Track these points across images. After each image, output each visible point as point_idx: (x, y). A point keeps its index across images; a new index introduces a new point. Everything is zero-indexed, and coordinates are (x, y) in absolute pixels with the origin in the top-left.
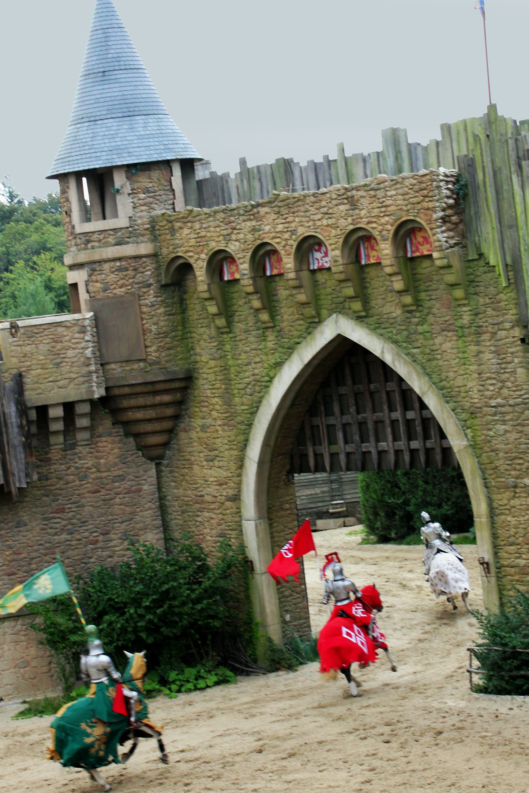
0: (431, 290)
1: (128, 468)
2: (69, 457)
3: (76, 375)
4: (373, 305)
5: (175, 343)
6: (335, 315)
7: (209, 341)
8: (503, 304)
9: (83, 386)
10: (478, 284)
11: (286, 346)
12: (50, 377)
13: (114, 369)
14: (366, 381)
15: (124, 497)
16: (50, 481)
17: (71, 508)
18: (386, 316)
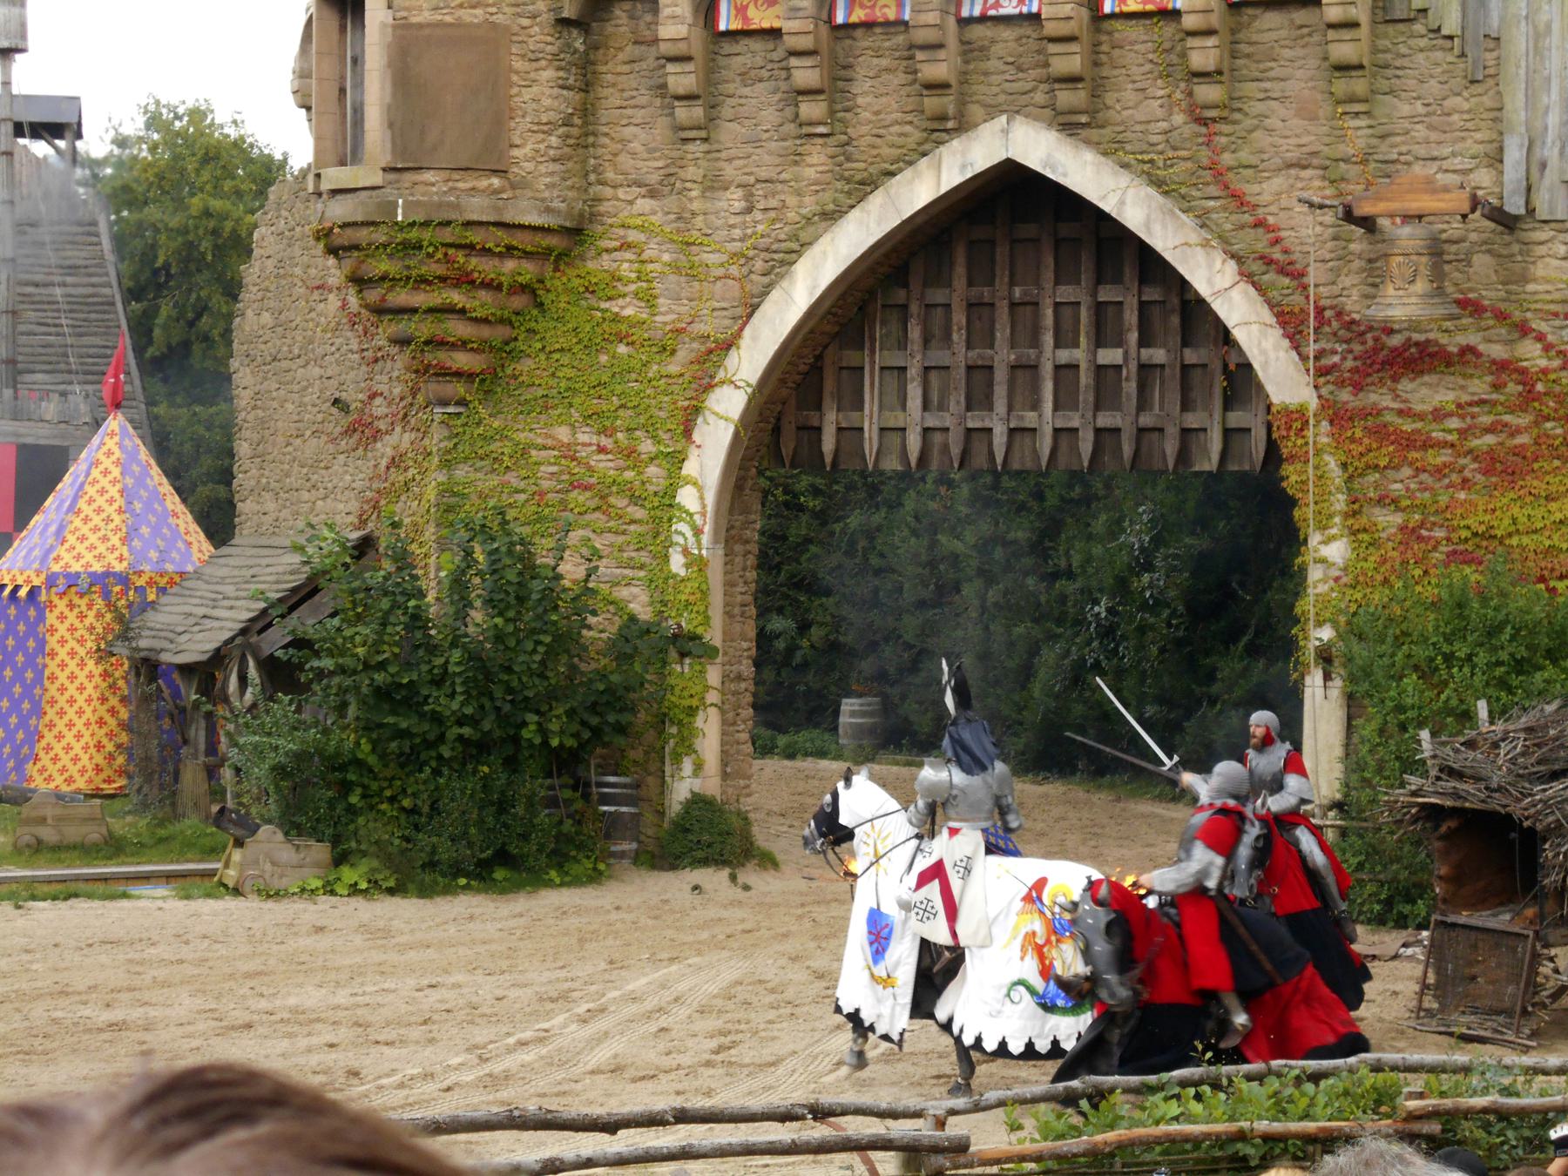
0: (1269, 80)
4: (1109, 102)
5: (567, 150)
6: (1004, 118)
7: (645, 156)
8: (1456, 117)
10: (1399, 73)
11: (858, 177)
14: (1006, 279)
18: (1138, 128)
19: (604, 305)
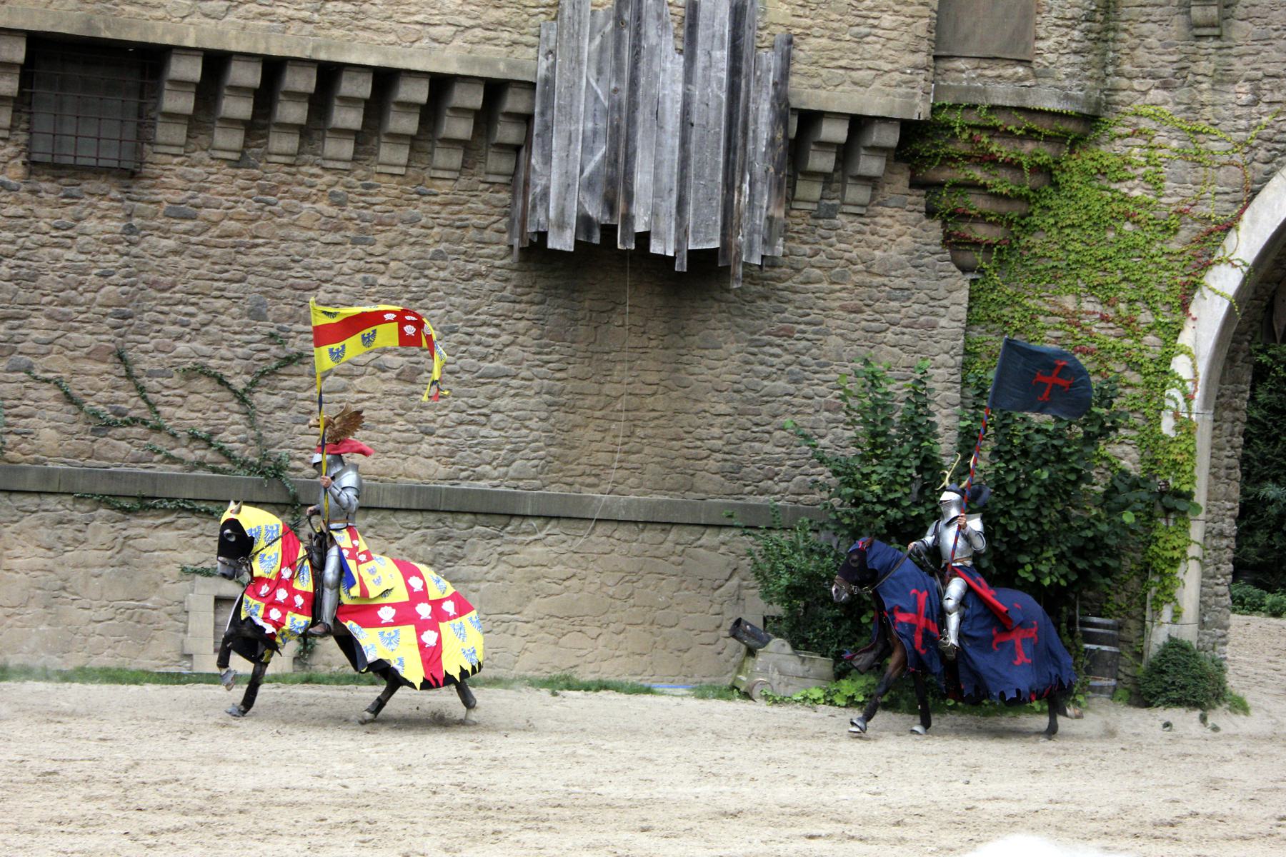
1: (921, 277)
2: (822, 232)
3: (888, 67)
5: (1087, 43)
7: (1161, 50)
9: (899, 90)
12: (841, 58)
13: (963, 71)
15: (903, 334)
16: (777, 270)
17: (804, 332)
19: (1113, 186)
